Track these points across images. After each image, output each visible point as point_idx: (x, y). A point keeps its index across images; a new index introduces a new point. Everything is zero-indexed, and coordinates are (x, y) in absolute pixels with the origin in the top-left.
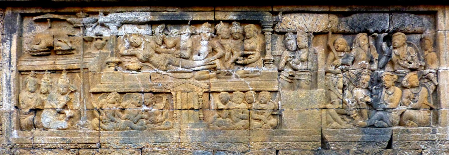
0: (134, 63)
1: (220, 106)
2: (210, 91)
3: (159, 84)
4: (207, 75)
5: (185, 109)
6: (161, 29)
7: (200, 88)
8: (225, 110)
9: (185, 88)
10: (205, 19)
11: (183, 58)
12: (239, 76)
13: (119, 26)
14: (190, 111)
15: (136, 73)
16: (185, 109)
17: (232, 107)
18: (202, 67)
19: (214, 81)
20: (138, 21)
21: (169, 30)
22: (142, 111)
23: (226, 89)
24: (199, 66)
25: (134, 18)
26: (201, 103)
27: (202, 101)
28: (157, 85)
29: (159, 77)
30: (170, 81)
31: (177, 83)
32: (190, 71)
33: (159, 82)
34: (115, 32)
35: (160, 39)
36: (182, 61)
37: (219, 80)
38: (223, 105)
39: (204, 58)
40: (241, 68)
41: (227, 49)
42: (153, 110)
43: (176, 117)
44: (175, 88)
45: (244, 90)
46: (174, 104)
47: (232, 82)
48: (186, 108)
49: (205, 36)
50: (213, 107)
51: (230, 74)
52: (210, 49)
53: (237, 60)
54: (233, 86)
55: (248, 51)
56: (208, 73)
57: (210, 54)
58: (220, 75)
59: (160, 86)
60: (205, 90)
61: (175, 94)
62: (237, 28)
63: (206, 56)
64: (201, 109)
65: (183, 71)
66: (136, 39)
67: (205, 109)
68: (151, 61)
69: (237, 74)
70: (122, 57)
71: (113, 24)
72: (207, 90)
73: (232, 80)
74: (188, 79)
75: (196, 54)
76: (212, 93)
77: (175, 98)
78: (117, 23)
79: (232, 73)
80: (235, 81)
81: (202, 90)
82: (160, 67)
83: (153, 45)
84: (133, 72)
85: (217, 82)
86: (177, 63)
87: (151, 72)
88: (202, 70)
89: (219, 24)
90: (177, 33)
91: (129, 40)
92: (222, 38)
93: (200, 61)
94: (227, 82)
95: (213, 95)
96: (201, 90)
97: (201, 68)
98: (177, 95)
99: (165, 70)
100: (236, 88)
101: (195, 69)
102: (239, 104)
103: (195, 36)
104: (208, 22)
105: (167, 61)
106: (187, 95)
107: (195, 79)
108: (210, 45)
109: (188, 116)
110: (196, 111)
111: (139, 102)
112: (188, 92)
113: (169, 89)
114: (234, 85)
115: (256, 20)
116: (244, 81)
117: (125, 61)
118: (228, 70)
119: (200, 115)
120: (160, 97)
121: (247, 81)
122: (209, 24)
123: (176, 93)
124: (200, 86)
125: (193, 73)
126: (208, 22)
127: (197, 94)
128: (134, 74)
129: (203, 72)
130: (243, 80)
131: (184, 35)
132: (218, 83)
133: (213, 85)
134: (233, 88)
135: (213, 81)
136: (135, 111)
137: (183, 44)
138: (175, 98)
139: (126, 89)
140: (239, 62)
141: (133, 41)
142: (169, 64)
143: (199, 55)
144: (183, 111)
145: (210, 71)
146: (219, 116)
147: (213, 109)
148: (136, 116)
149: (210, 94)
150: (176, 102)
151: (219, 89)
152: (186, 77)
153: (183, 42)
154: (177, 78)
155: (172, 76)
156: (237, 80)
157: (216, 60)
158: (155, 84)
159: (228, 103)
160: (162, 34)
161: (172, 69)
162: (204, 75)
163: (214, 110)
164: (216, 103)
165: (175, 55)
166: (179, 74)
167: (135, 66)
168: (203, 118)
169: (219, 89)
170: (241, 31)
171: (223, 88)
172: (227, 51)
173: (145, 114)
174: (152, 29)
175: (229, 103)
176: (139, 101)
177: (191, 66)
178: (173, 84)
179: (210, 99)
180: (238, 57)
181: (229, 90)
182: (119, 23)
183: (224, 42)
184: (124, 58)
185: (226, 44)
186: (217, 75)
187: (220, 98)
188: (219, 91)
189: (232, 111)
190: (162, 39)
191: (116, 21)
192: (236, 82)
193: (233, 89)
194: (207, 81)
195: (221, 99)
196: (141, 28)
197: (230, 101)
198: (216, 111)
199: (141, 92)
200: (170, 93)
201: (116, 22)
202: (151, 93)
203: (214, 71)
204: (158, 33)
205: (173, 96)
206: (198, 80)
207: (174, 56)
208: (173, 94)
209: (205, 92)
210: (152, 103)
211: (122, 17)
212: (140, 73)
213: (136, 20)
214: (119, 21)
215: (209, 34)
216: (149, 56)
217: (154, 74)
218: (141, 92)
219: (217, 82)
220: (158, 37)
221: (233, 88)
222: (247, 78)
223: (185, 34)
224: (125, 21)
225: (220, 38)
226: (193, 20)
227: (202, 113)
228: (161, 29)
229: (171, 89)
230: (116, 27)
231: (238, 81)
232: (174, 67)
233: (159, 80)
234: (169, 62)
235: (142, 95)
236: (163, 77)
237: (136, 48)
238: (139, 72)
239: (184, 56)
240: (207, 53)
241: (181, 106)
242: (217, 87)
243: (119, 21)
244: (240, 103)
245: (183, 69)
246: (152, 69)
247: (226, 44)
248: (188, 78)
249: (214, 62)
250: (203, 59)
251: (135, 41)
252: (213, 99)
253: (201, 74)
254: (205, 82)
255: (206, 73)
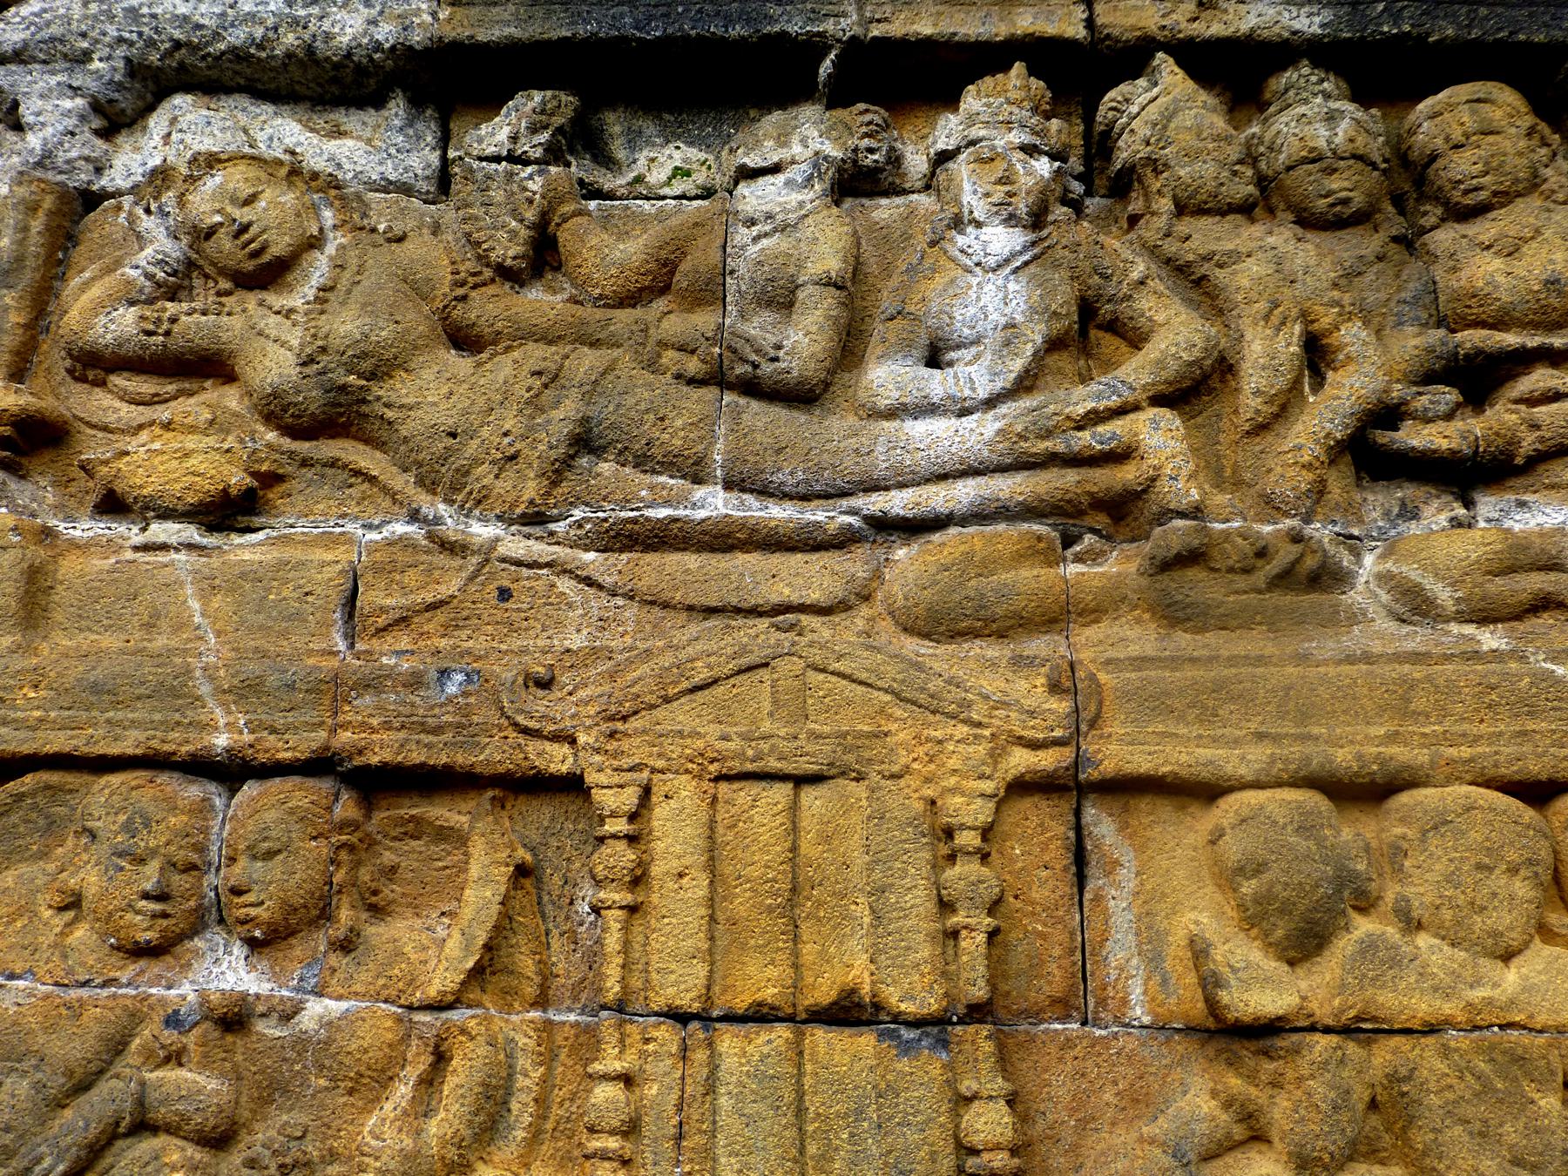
0: (192, 429)
1: (1246, 985)
2: (1089, 774)
3: (444, 673)
4: (1030, 578)
5: (761, 1015)
6: (534, 129)
7: (963, 730)
8: (1322, 1042)
9: (766, 726)
10: (995, 28)
11: (752, 388)
12: (1444, 595)
13: (126, 102)
14: (820, 1036)
15: (191, 547)
16: (761, 1015)
17: (1423, 1007)
18: (980, 480)
19: (1134, 650)
20: (310, 50)
21: (621, 154)
22: (173, 1021)
23: (1295, 751)
24: (943, 477)
25: (270, 23)
26: (981, 938)
27: (994, 908)
28: (415, 682)
29: (450, 586)
30: (577, 641)
31: (667, 660)
32: (832, 528)
33: (443, 643)
34: (74, 154)
35: (515, 213)
36: (737, 414)
37: (1183, 640)
38: (1272, 966)
39: (999, 385)
40: (1437, 513)
41: (1262, 306)
42: (316, 1009)
43: (631, 1129)
44: (635, 724)
45: (1536, 767)
46: (613, 941)
47: (1368, 658)
48: (770, 993)
49: (1000, 181)
50: (1136, 993)
51: (1323, 566)
52: (1064, 297)
53: (1388, 414)
54: (1382, 710)
55: (1499, 324)
56: (1053, 561)
57: (1061, 360)
58: (1197, 585)
59: (452, 689)
60: (1021, 761)
61: (629, 797)
62: (1331, 118)
63: (1017, 365)
64: (977, 1013)
65: (743, 524)
66: (250, 201)
67: (1035, 1015)
68: (389, 414)
69: (1412, 572)
70: (80, 387)
71: (54, 80)
72: (1047, 760)
73: (1355, 639)
74: (805, 619)
75: (905, 346)
76: (1116, 804)
77: (621, 856)
78: (96, 65)
79: (1346, 560)
80: (1400, 658)
81: (996, 756)
82: (483, 474)
83: (427, 265)
84: (162, 531)
85: (1175, 662)
86: (674, 438)
87: (373, 536)
88: (980, 515)
89: (1142, 82)
90: (700, 177)
91: (181, 201)
92: (1182, 209)
93: (954, 422)
94: (1303, 659)
95: (1123, 827)
96: (982, 749)
97: (964, 493)
98: (661, 813)
99: (535, 519)
100: (1429, 741)
101: (897, 503)
102: (1507, 957)
103: (884, 201)
104: (1018, 68)
105: (564, 414)
106: (794, 808)
107: (886, 626)
108: (1056, 266)
109: (800, 1112)
110: (907, 1048)
111: (146, 896)
112: (801, 781)
113: (556, 738)
114: (1401, 706)
115: (1540, 38)
116: (1523, 659)
117: (111, 418)
118: (1289, 523)
119: (969, 1100)
120: (444, 834)
121: (1553, 660)
122: (1037, 84)
123: (647, 791)
124: (966, 705)
125: (862, 551)
126: (1018, 68)
127: (919, 806)
128: (164, 547)
129: (990, 540)
130: (1490, 639)
131: (770, 179)
132: (1191, 673)
133: (1126, 695)
134: (1392, 738)
135: (1112, 654)
136: (76, 1010)
137: (753, 250)
138: (621, 856)
139: (18, 724)
140: (1414, 437)
141: (218, 218)
142: (585, 442)
143: (934, 359)
144: (729, 1041)
145: (1068, 541)
146: (1239, 1132)
147: (1140, 1013)
148: (83, 1087)
149: (1090, 813)
150: (633, 909)
151: (1205, 753)
152: (775, 599)
153: (755, 230)
154: (666, 606)
155: (608, 580)
156: (1417, 638)
157: (1136, 408)
158: (390, 674)
159: (1343, 946)
160: (540, 172)
161: (624, 503)
162: (1006, 577)
163: (1159, 1027)
164: (1178, 938)
165: (669, 357)
166: (692, 560)
167: (192, 462)
168: (1014, 1152)
169: (1205, 753)
170: (1376, 148)
171: (1260, 736)
172: (1267, 318)
173: (205, 1064)
174: (444, 141)
175: (1357, 934)
176: (149, 878)
177: (851, 467)
178: (612, 676)
179: (1081, 880)
180: (1398, 391)
181: (1343, 758)
182: (120, 64)
183: (1204, 236)
184: (98, 393)
185: (1235, 257)
186: (1165, 580)
187: (1229, 877)
188: (1205, 774)
189: (1427, 1058)
190: (530, 215)
191: (85, 45)
192: (1418, 672)
193: (1400, 754)
194: (1038, 646)
195: (1248, 887)
196: (338, 133)
197: (1362, 910)
198: (1181, 1045)
199: (200, 767)
200: (574, 785)
201: (86, 57)
202: (325, 785)
203: (1109, 538)
204: (497, 159)
205: (611, 827)
206: (927, 636)
207: (652, 365)
208: (614, 798)
209: (1021, 787)
210: (325, 914)
211: (154, 16)
212: (246, 549)
213: (289, 39)
214: (121, 52)
215: (1044, 167)
216: (366, 365)
217: (403, 558)
218: (200, 767)
219: (1175, 662)
220: (497, 195)
221: (1392, 738)
222: (1546, 619)
223: (775, 169)
224: (177, 45)
225: (1165, 204)
226: (876, 33)
227: (999, 1084)
228: (534, 129)
229: (582, 739)
230: (79, 102)
231: (1448, 658)
232: (641, 483)
233: (448, 629)
234: (585, 421)
235: (218, 802)
236: (505, 594)
237: (251, 299)
238: (237, 539)
239: (767, 368)
240: (1036, 335)
241: (701, 970)
242: (1181, 718)
243: (121, 52)
244: (1514, 938)
245: (749, 499)
246: (387, 503)
247: (1235, 257)
248: (803, 608)
249: (1117, 426)
250: (982, 394)
251: (243, 215)
252: (1126, 875)
253: (968, 557)
254: (1020, 663)
255: (1019, 558)
